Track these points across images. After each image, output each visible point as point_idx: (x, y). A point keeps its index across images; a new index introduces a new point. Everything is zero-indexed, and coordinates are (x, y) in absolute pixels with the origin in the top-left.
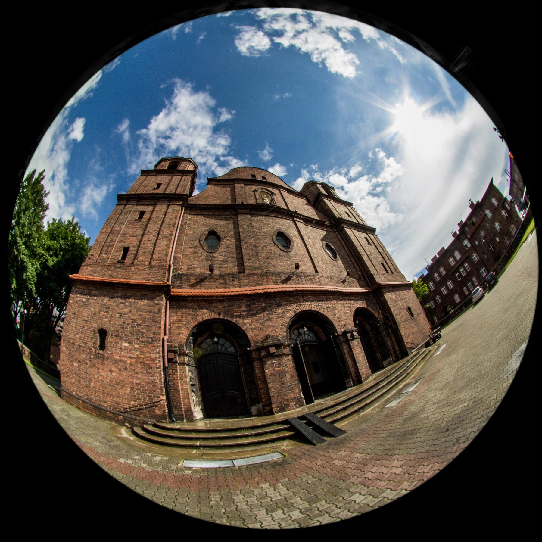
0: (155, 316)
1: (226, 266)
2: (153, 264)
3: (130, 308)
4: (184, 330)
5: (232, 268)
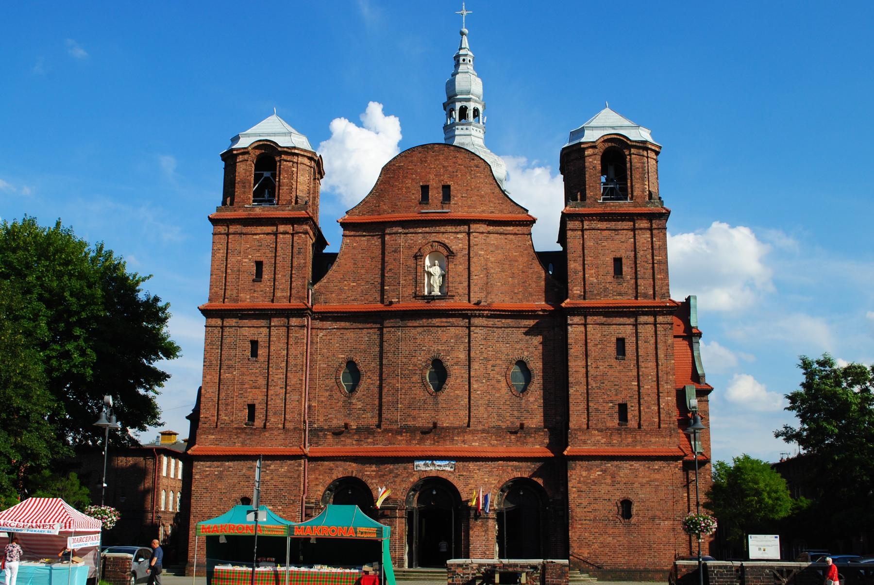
1: (364, 416)
2: (288, 425)
3: (272, 476)
5: (370, 419)
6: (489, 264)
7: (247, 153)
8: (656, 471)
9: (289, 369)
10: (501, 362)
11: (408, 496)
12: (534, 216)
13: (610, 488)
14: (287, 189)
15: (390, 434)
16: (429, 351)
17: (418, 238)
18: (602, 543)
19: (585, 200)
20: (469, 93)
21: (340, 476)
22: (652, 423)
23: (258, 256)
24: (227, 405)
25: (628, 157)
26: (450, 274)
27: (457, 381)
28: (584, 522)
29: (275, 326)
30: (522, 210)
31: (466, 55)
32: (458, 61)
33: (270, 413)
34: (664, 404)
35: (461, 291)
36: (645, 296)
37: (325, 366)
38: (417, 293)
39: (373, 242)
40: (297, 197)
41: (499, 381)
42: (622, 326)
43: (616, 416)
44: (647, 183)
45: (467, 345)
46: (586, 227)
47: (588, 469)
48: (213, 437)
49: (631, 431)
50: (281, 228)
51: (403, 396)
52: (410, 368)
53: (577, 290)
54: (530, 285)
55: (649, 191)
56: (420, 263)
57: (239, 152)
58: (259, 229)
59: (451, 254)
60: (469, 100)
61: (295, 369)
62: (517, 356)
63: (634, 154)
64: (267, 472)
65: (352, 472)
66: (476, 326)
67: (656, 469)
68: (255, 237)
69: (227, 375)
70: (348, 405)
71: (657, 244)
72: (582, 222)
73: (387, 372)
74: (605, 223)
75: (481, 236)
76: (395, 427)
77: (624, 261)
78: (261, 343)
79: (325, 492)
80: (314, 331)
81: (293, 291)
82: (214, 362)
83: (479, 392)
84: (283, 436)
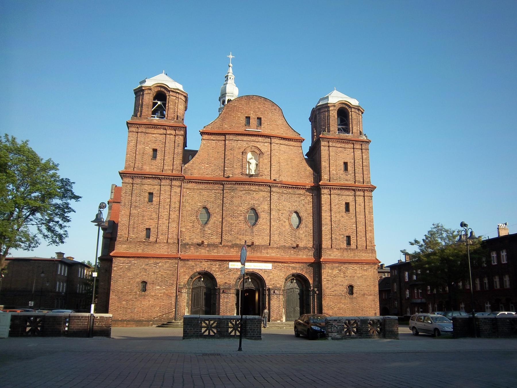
0: (173, 273)
1: (212, 238)
2: (169, 241)
4: (187, 276)
6: (281, 160)
7: (150, 89)
8: (365, 271)
9: (171, 210)
10: (286, 212)
11: (236, 282)
12: (304, 138)
13: (343, 279)
14: (172, 111)
15: (227, 248)
16: (249, 204)
17: (243, 143)
18: (339, 308)
19: (330, 132)
21: (198, 270)
22: (362, 246)
23: (154, 146)
24: (134, 228)
25: (350, 113)
26: (261, 164)
27: (264, 220)
28: (330, 297)
29: (163, 185)
30: (297, 134)
33: (159, 234)
34: (368, 237)
35: (266, 173)
36: (359, 182)
37: (190, 209)
38: (243, 172)
39: (219, 144)
40: (177, 116)
41: (285, 222)
42: (348, 196)
43: (345, 242)
44: (359, 127)
45: (269, 202)
47: (332, 269)
48: (125, 246)
49: (353, 250)
50: (169, 132)
51: (234, 228)
52: (238, 213)
53: (326, 177)
54: (301, 173)
55: (360, 131)
56: (245, 157)
57: (146, 88)
58: (156, 131)
59: (261, 153)
61: (174, 210)
62: (294, 209)
64: (157, 267)
65: (205, 268)
66: (274, 192)
67: (365, 270)
68: (153, 135)
69: (134, 211)
70: (203, 231)
71: (364, 157)
73: (225, 214)
75: (277, 145)
76: (230, 244)
77: (349, 164)
78: (155, 194)
79: (189, 279)
80: (185, 190)
81: (175, 167)
82: (127, 203)
83: (275, 227)
84: (166, 247)
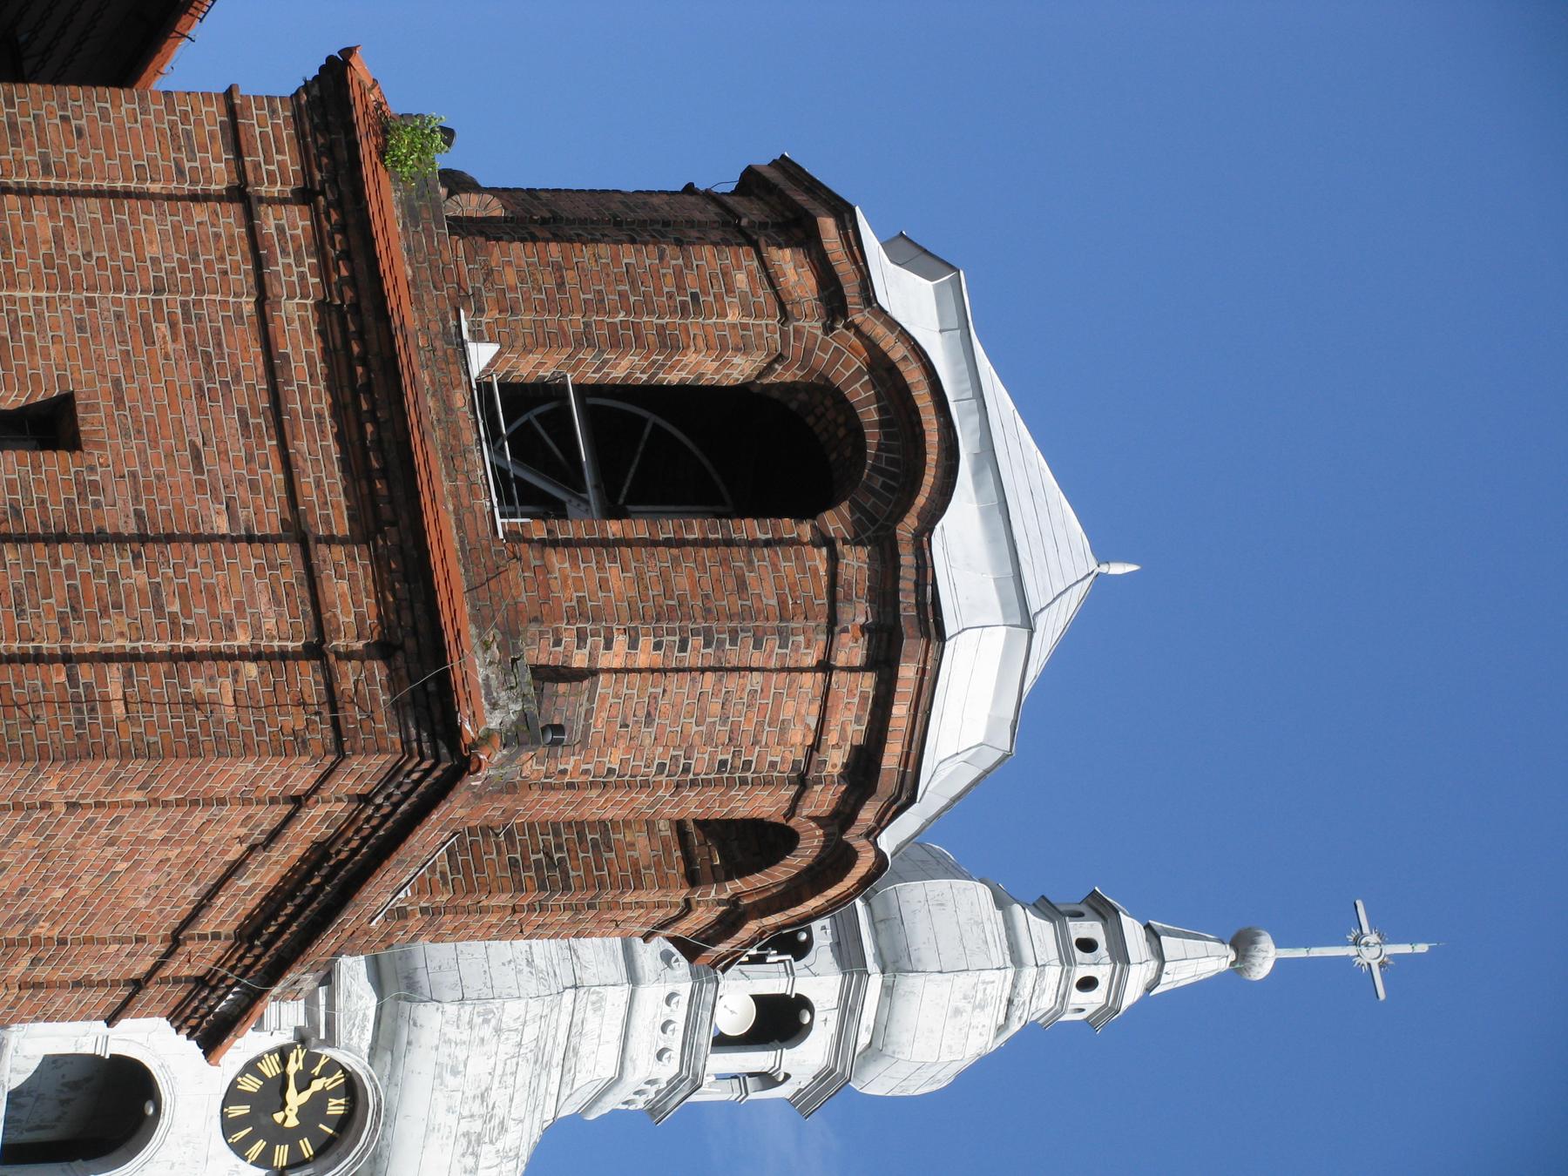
20: (896, 963)
25: (806, 530)
31: (1120, 954)
32: (1078, 915)
44: (643, 658)
46: (269, 221)
55: (592, 673)
60: (849, 957)
63: (834, 559)
72: (304, 196)
74: (315, 349)
77: (55, 463)
